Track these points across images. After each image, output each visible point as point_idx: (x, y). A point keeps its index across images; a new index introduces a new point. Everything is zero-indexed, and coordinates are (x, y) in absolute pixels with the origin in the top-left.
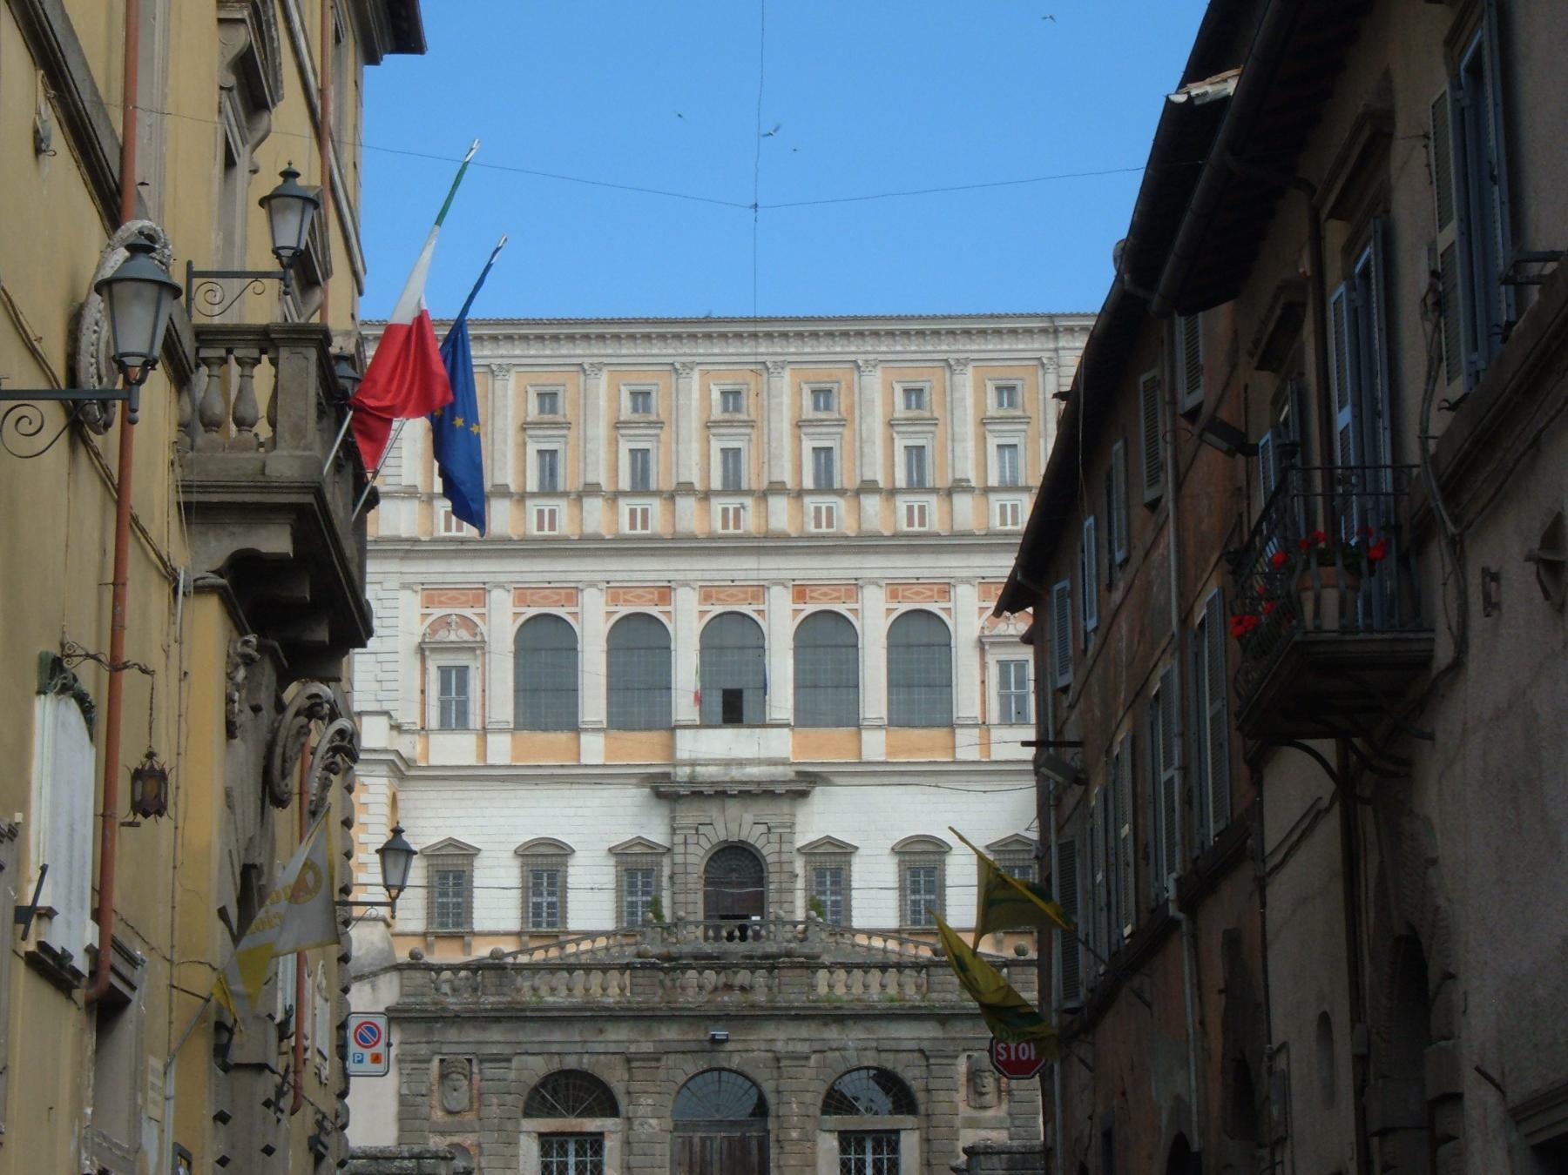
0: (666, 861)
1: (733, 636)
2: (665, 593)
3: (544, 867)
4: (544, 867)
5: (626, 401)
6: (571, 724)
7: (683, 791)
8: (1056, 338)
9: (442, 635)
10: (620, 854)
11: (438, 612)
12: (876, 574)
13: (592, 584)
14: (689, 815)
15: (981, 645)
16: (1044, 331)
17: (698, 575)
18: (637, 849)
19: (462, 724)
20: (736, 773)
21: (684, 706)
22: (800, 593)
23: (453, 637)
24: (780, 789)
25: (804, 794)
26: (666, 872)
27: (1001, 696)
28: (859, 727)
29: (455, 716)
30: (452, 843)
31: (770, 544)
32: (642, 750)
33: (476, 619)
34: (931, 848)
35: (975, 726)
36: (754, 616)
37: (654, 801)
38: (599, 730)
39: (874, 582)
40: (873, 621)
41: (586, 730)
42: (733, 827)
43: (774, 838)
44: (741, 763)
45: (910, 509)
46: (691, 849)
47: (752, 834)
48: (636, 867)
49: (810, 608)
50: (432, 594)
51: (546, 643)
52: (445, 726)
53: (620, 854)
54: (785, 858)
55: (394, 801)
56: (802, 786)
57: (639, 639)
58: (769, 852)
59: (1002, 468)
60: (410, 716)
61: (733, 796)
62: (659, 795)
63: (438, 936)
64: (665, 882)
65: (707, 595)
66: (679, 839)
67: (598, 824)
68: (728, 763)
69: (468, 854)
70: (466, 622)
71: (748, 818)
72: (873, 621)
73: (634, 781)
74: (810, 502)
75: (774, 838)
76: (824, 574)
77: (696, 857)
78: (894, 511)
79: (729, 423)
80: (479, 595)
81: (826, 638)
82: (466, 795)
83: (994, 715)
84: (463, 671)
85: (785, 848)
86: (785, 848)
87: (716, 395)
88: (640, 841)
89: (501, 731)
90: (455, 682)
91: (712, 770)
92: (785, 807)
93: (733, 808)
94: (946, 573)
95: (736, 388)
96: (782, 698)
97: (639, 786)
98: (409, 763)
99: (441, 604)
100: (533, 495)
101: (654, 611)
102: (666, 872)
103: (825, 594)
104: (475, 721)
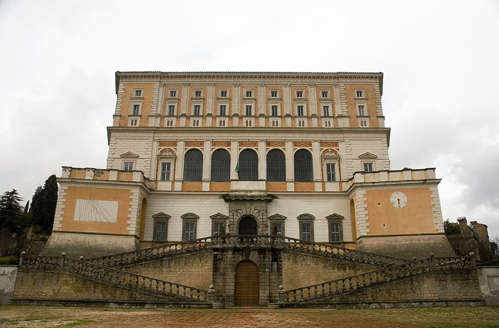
0: (228, 221)
1: (248, 158)
2: (229, 144)
3: (190, 221)
4: (190, 221)
5: (220, 93)
6: (200, 179)
7: (233, 199)
8: (338, 80)
9: (164, 154)
10: (213, 218)
11: (163, 148)
12: (291, 138)
13: (208, 140)
14: (236, 206)
15: (323, 158)
16: (335, 77)
17: (238, 138)
18: (218, 217)
19: (168, 179)
20: (249, 194)
21: (234, 175)
22: (268, 144)
23: (167, 154)
24: (263, 199)
25: (270, 201)
26: (228, 224)
27: (328, 174)
28: (285, 181)
29: (165, 177)
30: (162, 214)
31: (258, 130)
32: (221, 186)
33: (174, 150)
34: (309, 218)
35: (321, 182)
36: (255, 150)
37: (224, 203)
38: (208, 181)
39: (290, 141)
40: (289, 153)
41: (204, 181)
42: (248, 210)
43: (261, 214)
44: (251, 191)
45: (300, 122)
46: (235, 217)
47: (254, 213)
48: (218, 221)
49: (271, 148)
50: (161, 143)
51: (193, 157)
52: (163, 179)
53: (213, 218)
54: (265, 220)
55: (144, 202)
56: (269, 199)
57: (221, 158)
58: (259, 219)
59: (325, 114)
60: (153, 177)
61: (248, 201)
62: (226, 201)
63: (156, 242)
64: (227, 227)
65: (241, 143)
66: (231, 214)
67: (207, 209)
68: (247, 191)
69: (168, 218)
70: (171, 150)
71: (253, 208)
72: (289, 153)
73: (218, 196)
74: (271, 120)
75: (261, 214)
76: (276, 138)
77: (237, 219)
78: (295, 122)
79: (249, 99)
80: (175, 143)
81: (276, 158)
82: (168, 200)
83: (326, 179)
84: (169, 164)
85: (264, 217)
86: (264, 217)
87: (245, 92)
88: (218, 215)
89: (179, 181)
90: (166, 168)
91: (242, 193)
92: (264, 204)
93: (248, 205)
94: (311, 139)
95: (251, 90)
96: (262, 172)
97: (220, 198)
98: (151, 190)
99: (165, 145)
100: (193, 116)
101: (226, 148)
102: (228, 224)
103: (276, 144)
104: (171, 178)
